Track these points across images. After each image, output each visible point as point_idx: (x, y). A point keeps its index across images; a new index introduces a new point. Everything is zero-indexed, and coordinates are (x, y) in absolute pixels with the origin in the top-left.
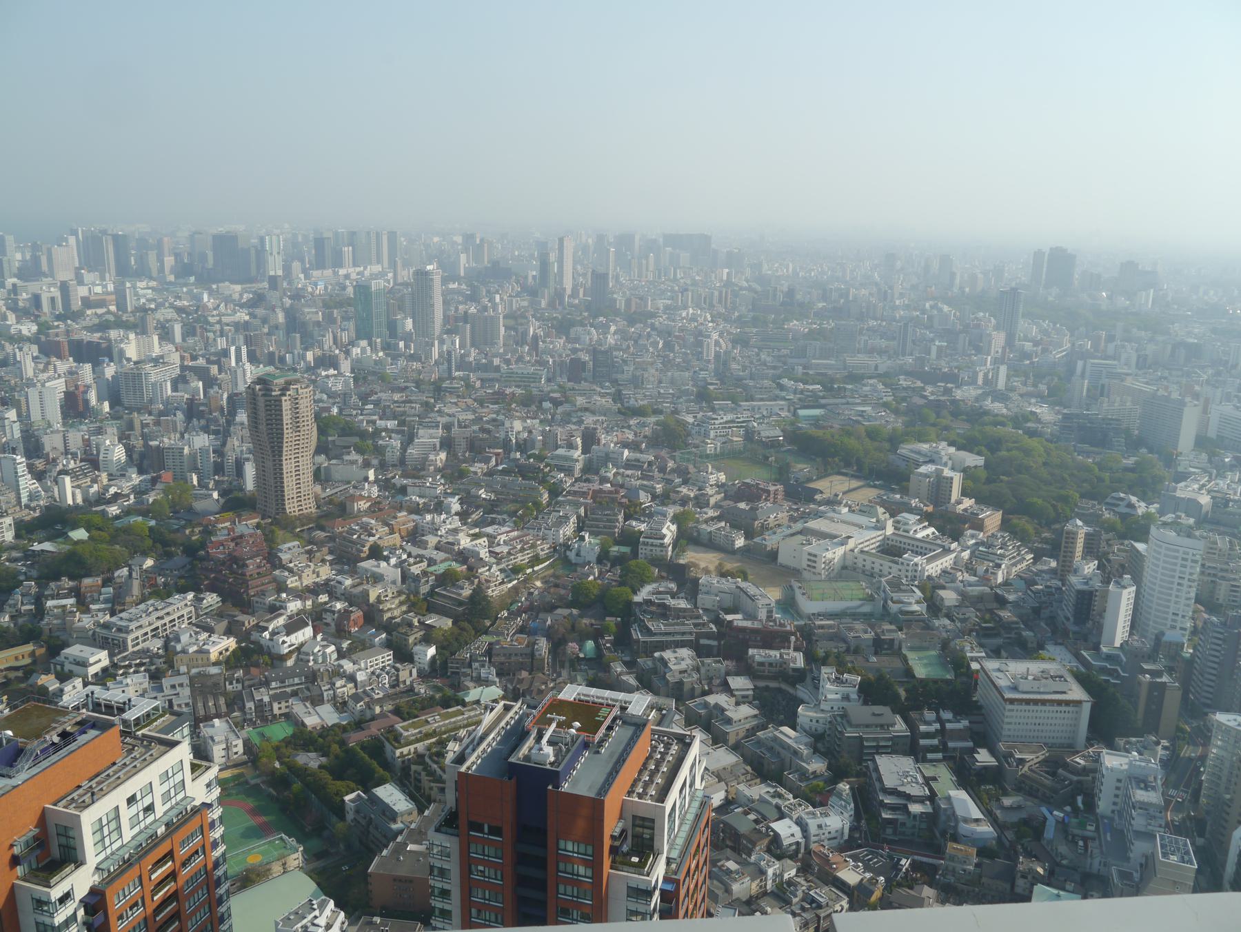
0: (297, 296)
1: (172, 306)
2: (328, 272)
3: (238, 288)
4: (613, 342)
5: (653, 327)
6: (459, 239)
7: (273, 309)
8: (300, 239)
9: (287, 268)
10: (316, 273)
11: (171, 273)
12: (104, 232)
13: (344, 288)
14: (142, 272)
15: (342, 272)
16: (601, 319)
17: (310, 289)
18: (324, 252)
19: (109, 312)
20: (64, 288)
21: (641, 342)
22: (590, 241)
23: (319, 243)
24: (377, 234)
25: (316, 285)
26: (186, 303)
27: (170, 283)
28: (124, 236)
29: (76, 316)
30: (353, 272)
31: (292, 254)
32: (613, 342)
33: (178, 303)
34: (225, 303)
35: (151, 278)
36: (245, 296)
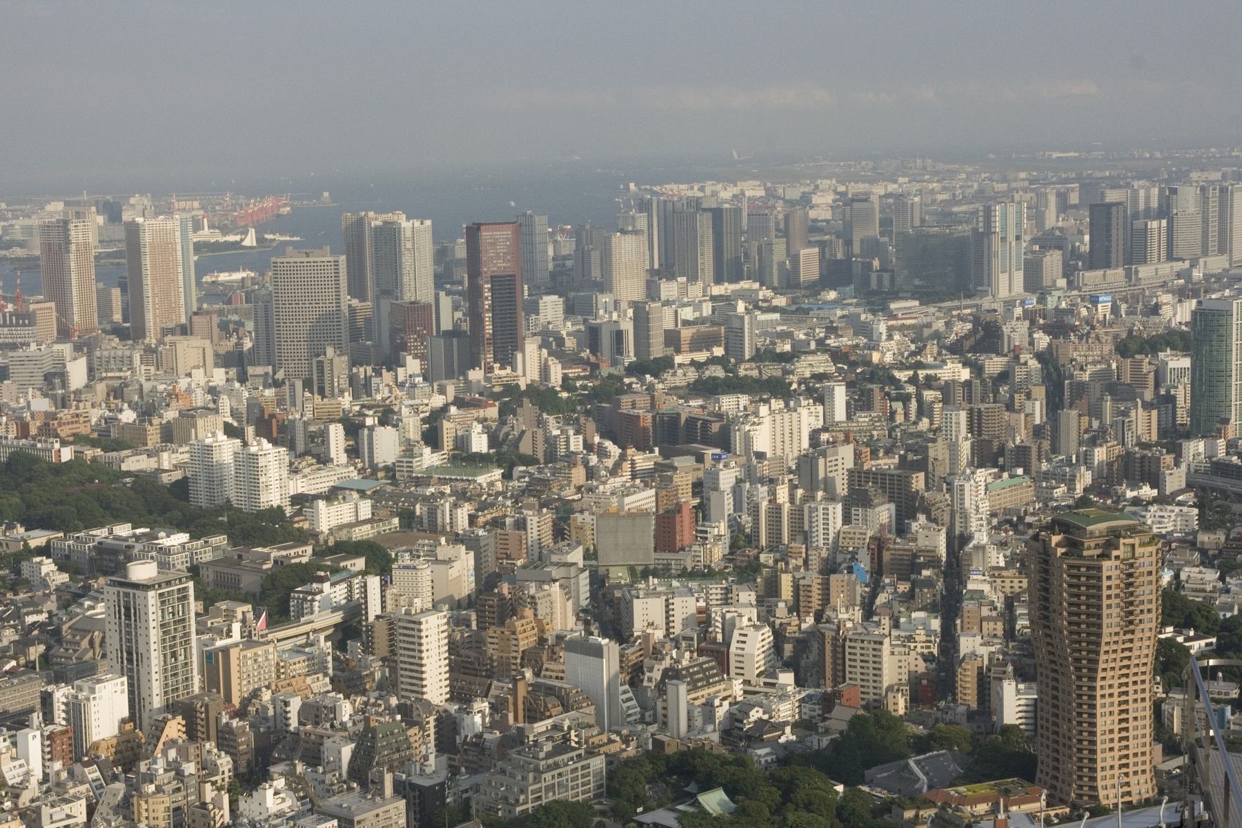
2: (1116, 274)
7: (1015, 355)
10: (1091, 277)
12: (696, 204)
15: (1145, 271)
17: (1084, 312)
25: (1094, 301)
26: (846, 341)
29: (661, 367)
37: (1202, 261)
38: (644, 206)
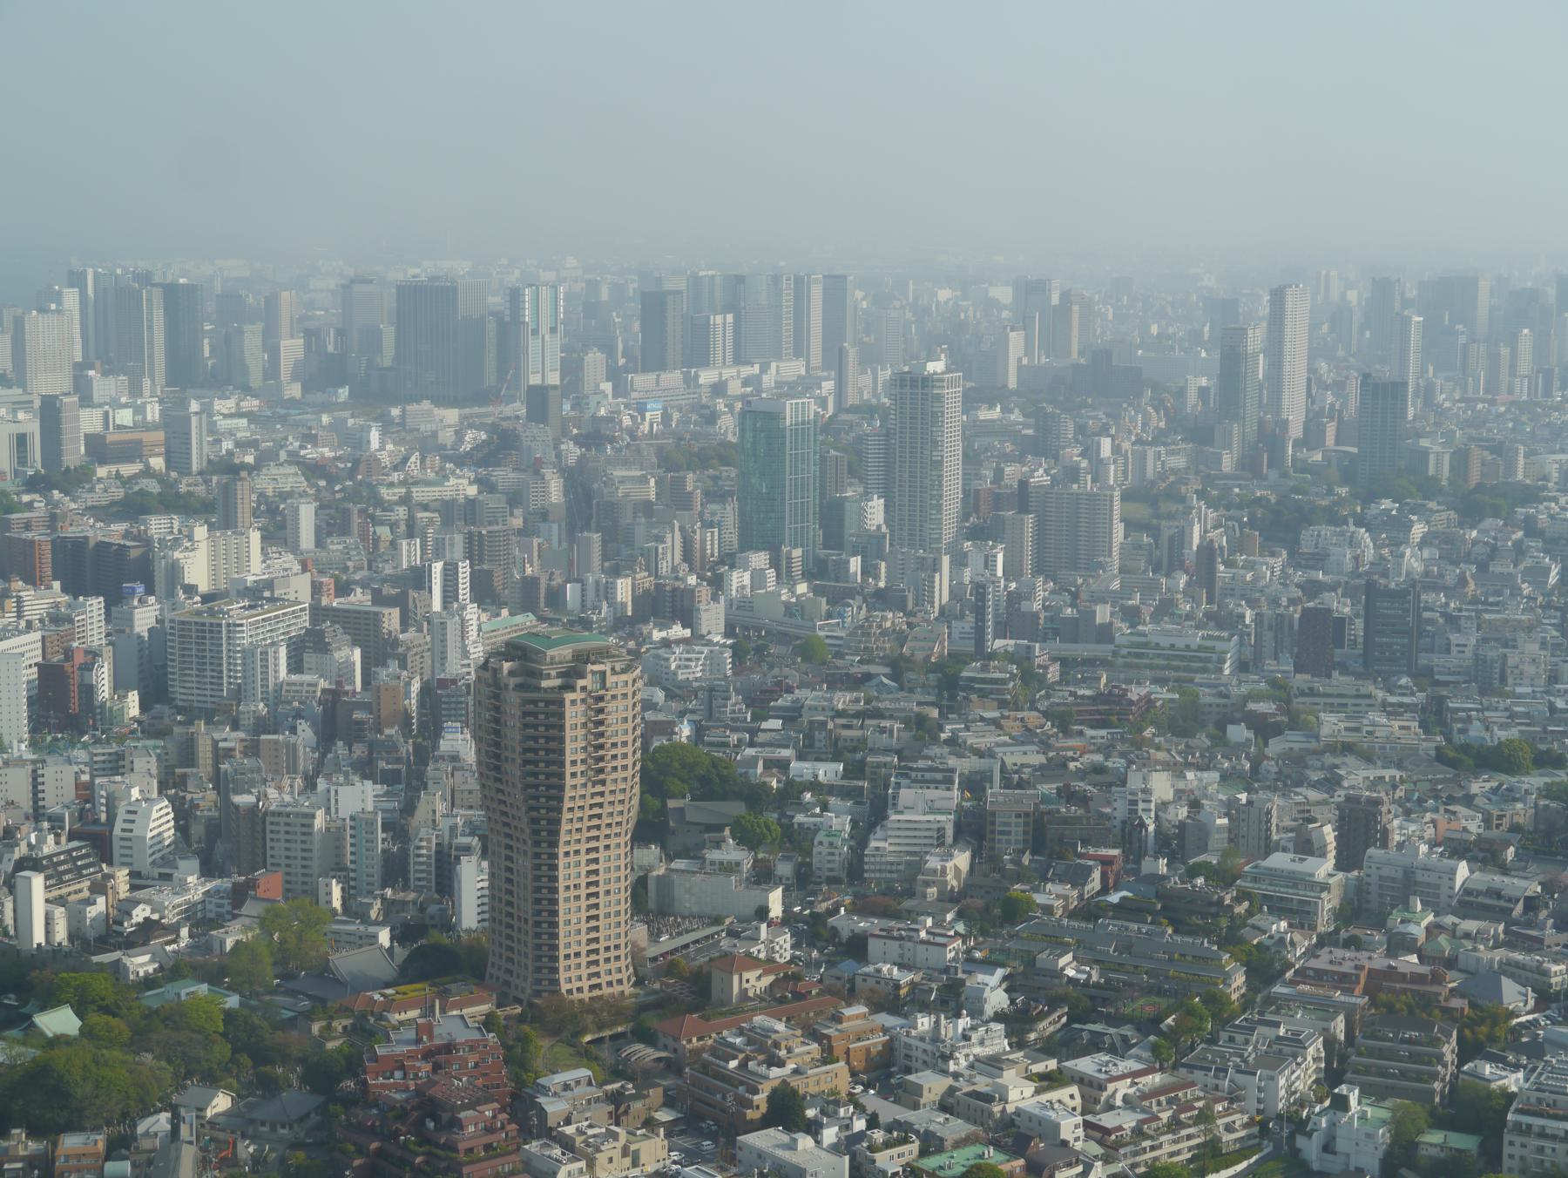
0: (594, 438)
1: (295, 459)
3: (452, 415)
4: (1418, 566)
5: (1531, 529)
6: (1003, 294)
7: (536, 468)
8: (605, 295)
9: (572, 368)
11: (294, 378)
12: (145, 279)
13: (712, 418)
14: (227, 377)
15: (707, 377)
16: (1386, 504)
17: (627, 421)
18: (664, 327)
19: (148, 472)
20: (50, 412)
21: (1496, 568)
22: (1352, 296)
23: (654, 306)
24: (799, 281)
25: (642, 410)
26: (327, 452)
27: (292, 401)
28: (191, 289)
29: (74, 480)
30: (734, 377)
31: (586, 331)
32: (1418, 566)
33: (309, 453)
34: (422, 452)
35: (247, 391)
36: (469, 436)
37: (773, 365)
38: (77, 280)
